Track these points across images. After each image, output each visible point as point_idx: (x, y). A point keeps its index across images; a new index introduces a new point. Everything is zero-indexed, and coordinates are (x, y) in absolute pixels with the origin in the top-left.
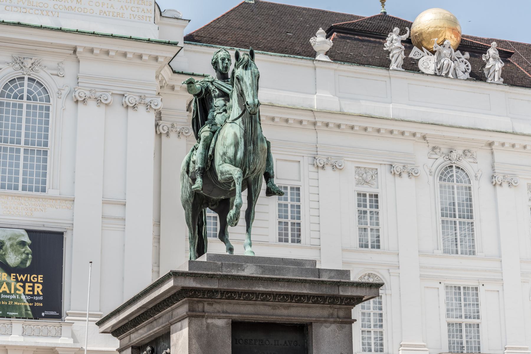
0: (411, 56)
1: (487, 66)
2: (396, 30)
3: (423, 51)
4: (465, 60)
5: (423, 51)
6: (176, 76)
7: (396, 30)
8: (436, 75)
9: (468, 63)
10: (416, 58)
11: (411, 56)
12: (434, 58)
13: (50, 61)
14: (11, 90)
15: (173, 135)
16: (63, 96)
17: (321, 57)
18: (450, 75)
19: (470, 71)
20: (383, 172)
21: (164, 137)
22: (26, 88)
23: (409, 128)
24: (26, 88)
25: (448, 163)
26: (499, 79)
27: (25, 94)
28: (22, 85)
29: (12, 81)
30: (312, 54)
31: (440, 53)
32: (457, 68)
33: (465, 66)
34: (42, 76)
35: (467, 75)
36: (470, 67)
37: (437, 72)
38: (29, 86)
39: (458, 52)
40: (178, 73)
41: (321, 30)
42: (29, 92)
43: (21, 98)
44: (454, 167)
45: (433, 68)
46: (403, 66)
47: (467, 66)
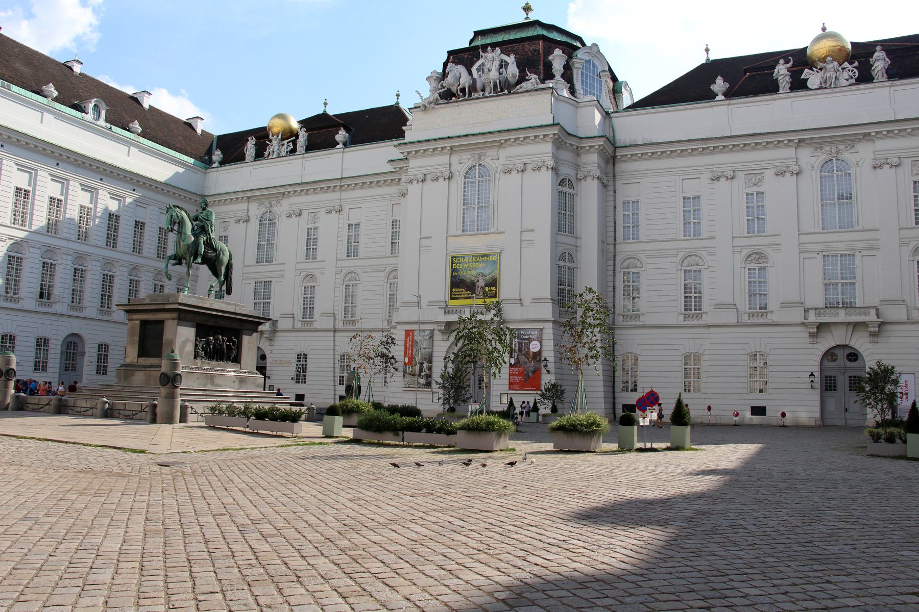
0: (802, 77)
1: (873, 68)
2: (782, 61)
3: (813, 70)
4: (851, 69)
5: (813, 70)
6: (583, 141)
7: (782, 61)
8: (820, 88)
9: (855, 70)
10: (807, 77)
11: (802, 77)
12: (821, 73)
13: (491, 153)
14: (470, 174)
15: (589, 179)
16: (499, 171)
17: (720, 97)
18: (833, 86)
19: (856, 76)
20: (769, 174)
21: (583, 181)
22: (477, 171)
23: (785, 138)
24: (477, 171)
25: (830, 157)
26: (883, 76)
27: (477, 174)
28: (475, 170)
29: (470, 169)
30: (712, 96)
31: (826, 69)
32: (840, 78)
33: (851, 74)
34: (487, 161)
35: (853, 81)
36: (857, 74)
37: (823, 86)
38: (479, 169)
39: (846, 63)
40: (585, 138)
41: (719, 77)
42: (479, 173)
43: (475, 177)
44: (834, 159)
45: (818, 82)
46: (790, 88)
47: (855, 73)
